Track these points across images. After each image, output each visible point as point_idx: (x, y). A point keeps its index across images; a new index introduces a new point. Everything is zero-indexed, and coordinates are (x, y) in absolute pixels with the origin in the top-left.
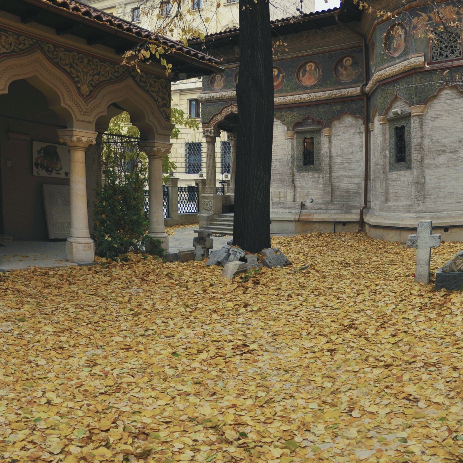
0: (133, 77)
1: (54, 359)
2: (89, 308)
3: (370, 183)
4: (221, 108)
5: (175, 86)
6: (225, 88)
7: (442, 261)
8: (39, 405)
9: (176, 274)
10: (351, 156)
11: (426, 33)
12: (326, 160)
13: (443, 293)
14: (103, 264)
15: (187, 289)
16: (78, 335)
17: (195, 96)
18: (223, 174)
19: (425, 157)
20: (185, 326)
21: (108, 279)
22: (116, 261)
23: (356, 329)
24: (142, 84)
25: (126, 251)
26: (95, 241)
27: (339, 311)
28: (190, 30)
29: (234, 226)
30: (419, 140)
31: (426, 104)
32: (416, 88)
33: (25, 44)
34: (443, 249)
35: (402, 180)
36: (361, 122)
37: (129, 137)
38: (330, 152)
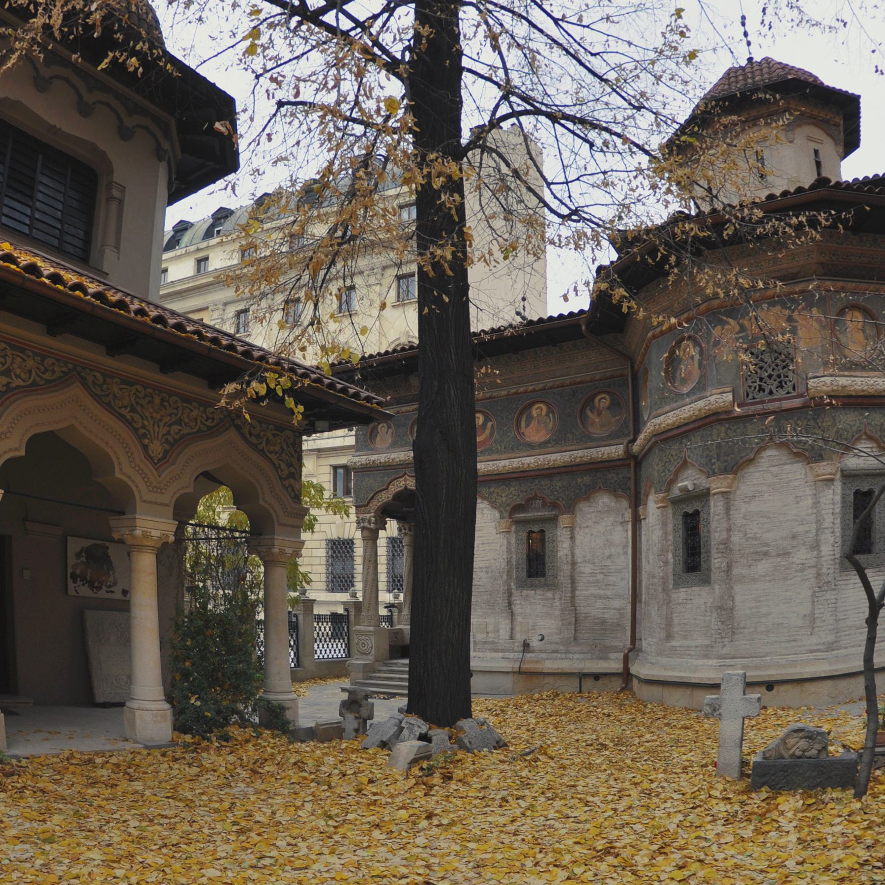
0: (238, 428)
2: (163, 821)
3: (641, 608)
4: (387, 479)
5: (310, 443)
6: (394, 445)
7: (763, 740)
9: (310, 762)
10: (608, 563)
11: (736, 353)
12: (566, 569)
13: (764, 795)
14: (186, 745)
15: (330, 787)
16: (145, 866)
17: (342, 460)
18: (389, 591)
19: (734, 565)
20: (326, 851)
21: (195, 770)
22: (209, 739)
23: (617, 855)
24: (254, 440)
25: (226, 722)
26: (173, 706)
27: (588, 826)
28: (334, 348)
29: (410, 680)
30: (724, 535)
31: (735, 473)
32: (719, 446)
33: (53, 372)
34: (765, 720)
35: (695, 601)
36: (625, 503)
37: (232, 530)
38: (573, 554)
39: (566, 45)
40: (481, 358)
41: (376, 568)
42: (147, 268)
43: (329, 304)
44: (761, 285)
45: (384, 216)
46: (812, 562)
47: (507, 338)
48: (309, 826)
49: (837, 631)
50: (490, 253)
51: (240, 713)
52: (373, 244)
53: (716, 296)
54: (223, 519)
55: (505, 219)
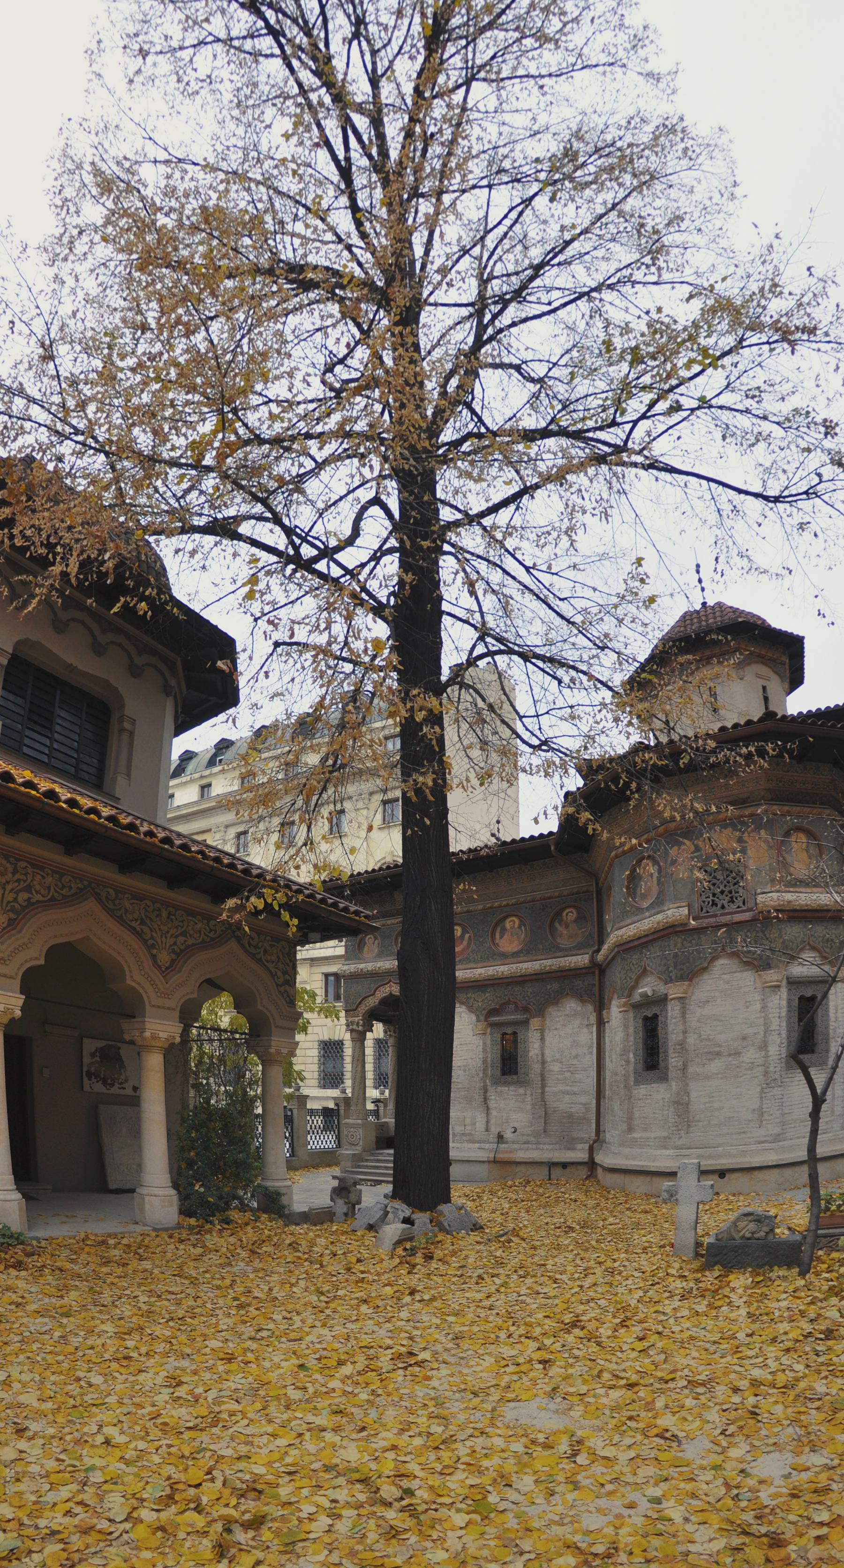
0: (239, 940)
1: (117, 1374)
2: (169, 1297)
4: (373, 986)
5: (304, 953)
6: (380, 955)
7: (716, 1223)
8: (93, 1446)
9: (304, 1243)
10: (575, 1062)
11: (691, 870)
12: (536, 1067)
13: (717, 1273)
14: (191, 1228)
15: (322, 1266)
16: (153, 1337)
17: (333, 969)
18: (376, 1088)
20: (318, 1324)
21: (199, 1251)
22: (211, 1223)
23: (583, 1328)
24: (253, 950)
25: (227, 1207)
26: (179, 1192)
27: (556, 1301)
28: (326, 866)
29: (394, 1169)
31: (691, 980)
32: (676, 955)
33: (70, 888)
34: (717, 1205)
35: (654, 1097)
36: (590, 1008)
37: (233, 1032)
38: (543, 1054)
39: (537, 591)
40: (459, 876)
41: (363, 1067)
42: (156, 794)
43: (321, 827)
44: (714, 809)
45: (371, 746)
46: (760, 1061)
47: (483, 857)
48: (303, 1301)
49: (783, 1124)
50: (468, 780)
51: (240, 1199)
52: (361, 772)
53: (673, 819)
54: (225, 1022)
55: (482, 749)
